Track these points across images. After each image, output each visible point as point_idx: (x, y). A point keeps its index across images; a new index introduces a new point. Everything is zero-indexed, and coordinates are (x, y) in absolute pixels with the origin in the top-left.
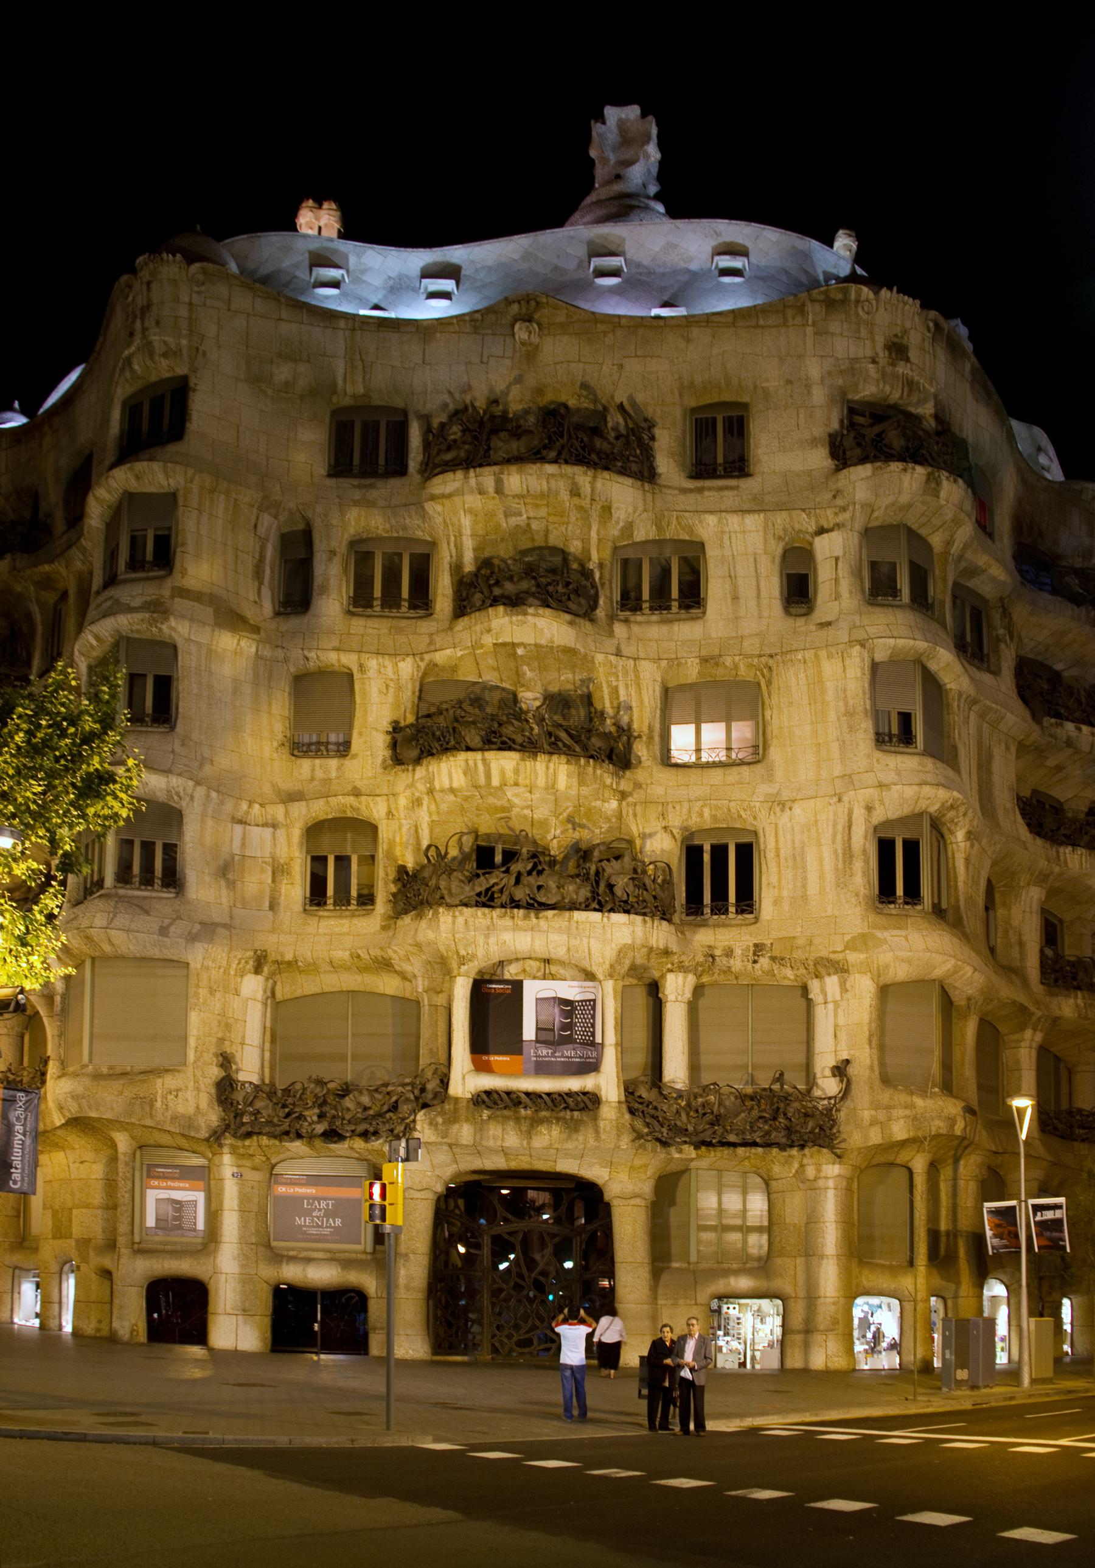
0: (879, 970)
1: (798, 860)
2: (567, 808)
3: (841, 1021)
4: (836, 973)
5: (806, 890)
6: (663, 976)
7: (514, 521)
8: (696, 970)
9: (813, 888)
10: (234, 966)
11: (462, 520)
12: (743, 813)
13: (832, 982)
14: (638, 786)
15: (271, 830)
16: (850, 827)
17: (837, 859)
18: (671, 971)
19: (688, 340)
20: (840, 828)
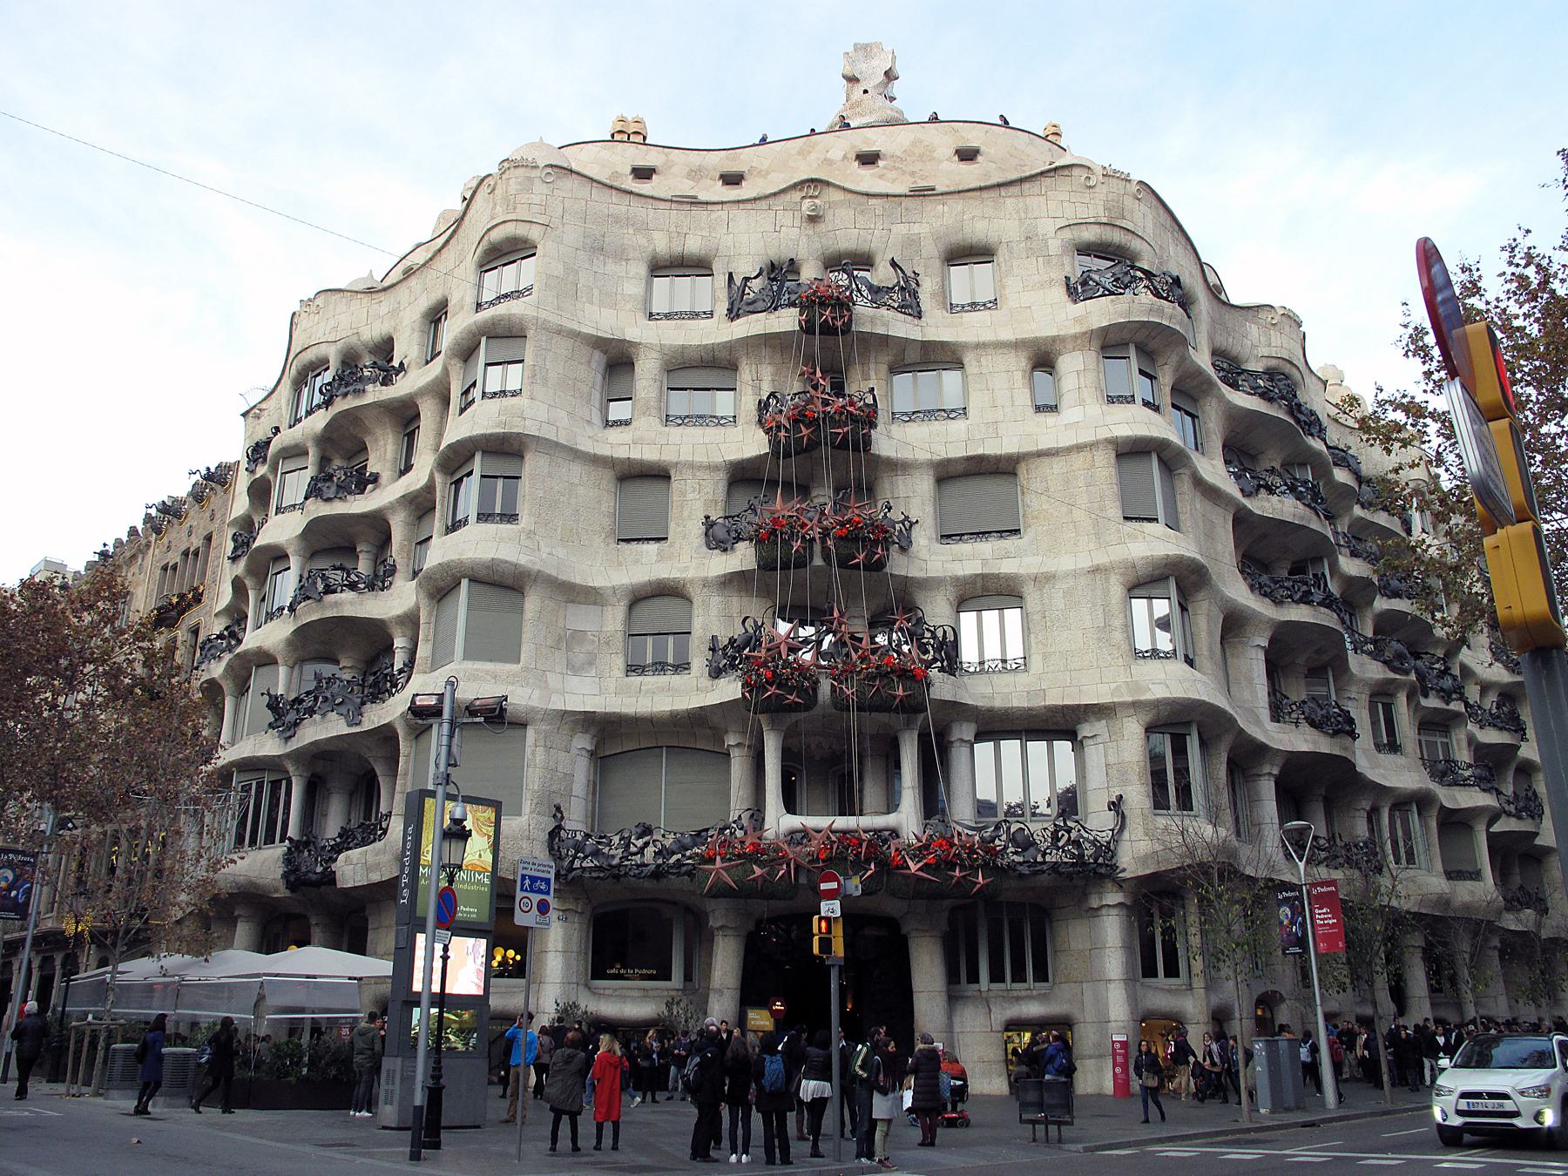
3: (1112, 760)
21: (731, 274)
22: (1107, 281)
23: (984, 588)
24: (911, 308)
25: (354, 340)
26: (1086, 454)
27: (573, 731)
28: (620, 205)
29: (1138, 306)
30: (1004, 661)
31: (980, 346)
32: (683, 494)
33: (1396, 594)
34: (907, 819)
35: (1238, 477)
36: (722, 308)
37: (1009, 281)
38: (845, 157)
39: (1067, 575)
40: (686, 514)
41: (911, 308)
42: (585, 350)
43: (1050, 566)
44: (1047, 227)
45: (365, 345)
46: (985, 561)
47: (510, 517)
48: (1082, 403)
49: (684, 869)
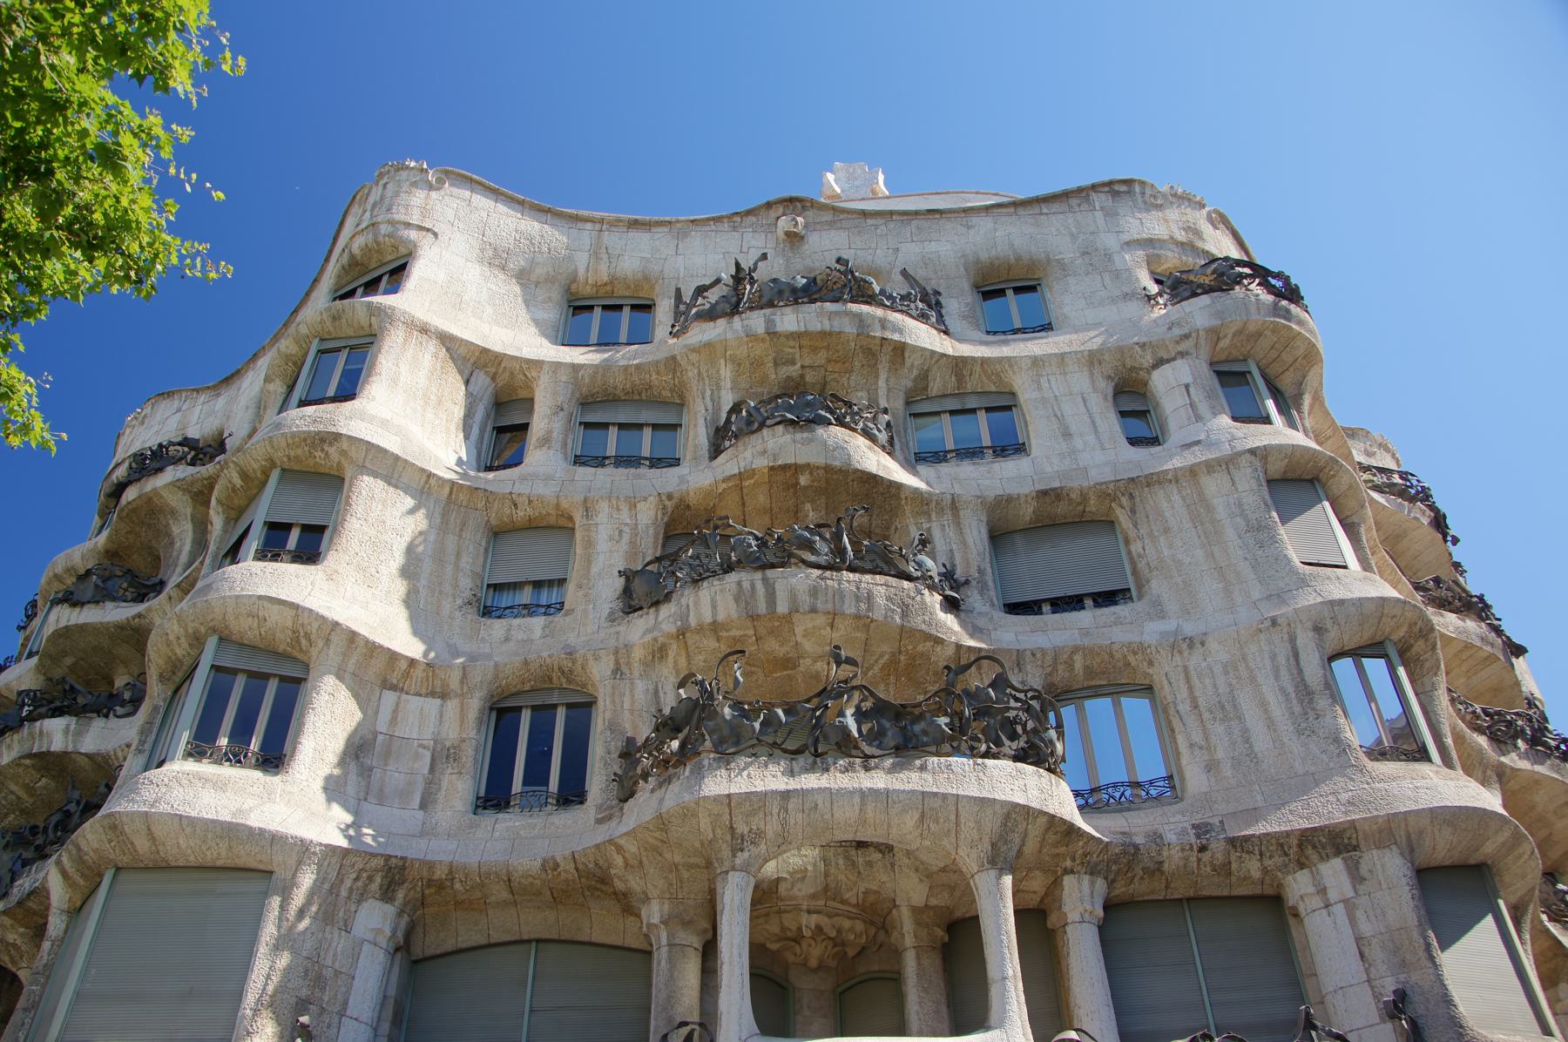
0: (1409, 837)
1: (1227, 710)
2: (881, 656)
3: (1366, 929)
4: (1338, 853)
5: (1251, 746)
6: (1057, 883)
8: (1109, 870)
9: (1262, 742)
10: (348, 883)
11: (722, 372)
12: (1131, 658)
13: (1333, 871)
15: (438, 701)
16: (1296, 656)
17: (1288, 700)
18: (1067, 871)
20: (1282, 660)
21: (678, 291)
23: (1089, 671)
27: (362, 897)
28: (532, 226)
30: (1136, 785)
31: (1036, 362)
32: (589, 544)
40: (594, 570)
44: (1110, 241)
46: (1085, 633)
48: (1198, 418)
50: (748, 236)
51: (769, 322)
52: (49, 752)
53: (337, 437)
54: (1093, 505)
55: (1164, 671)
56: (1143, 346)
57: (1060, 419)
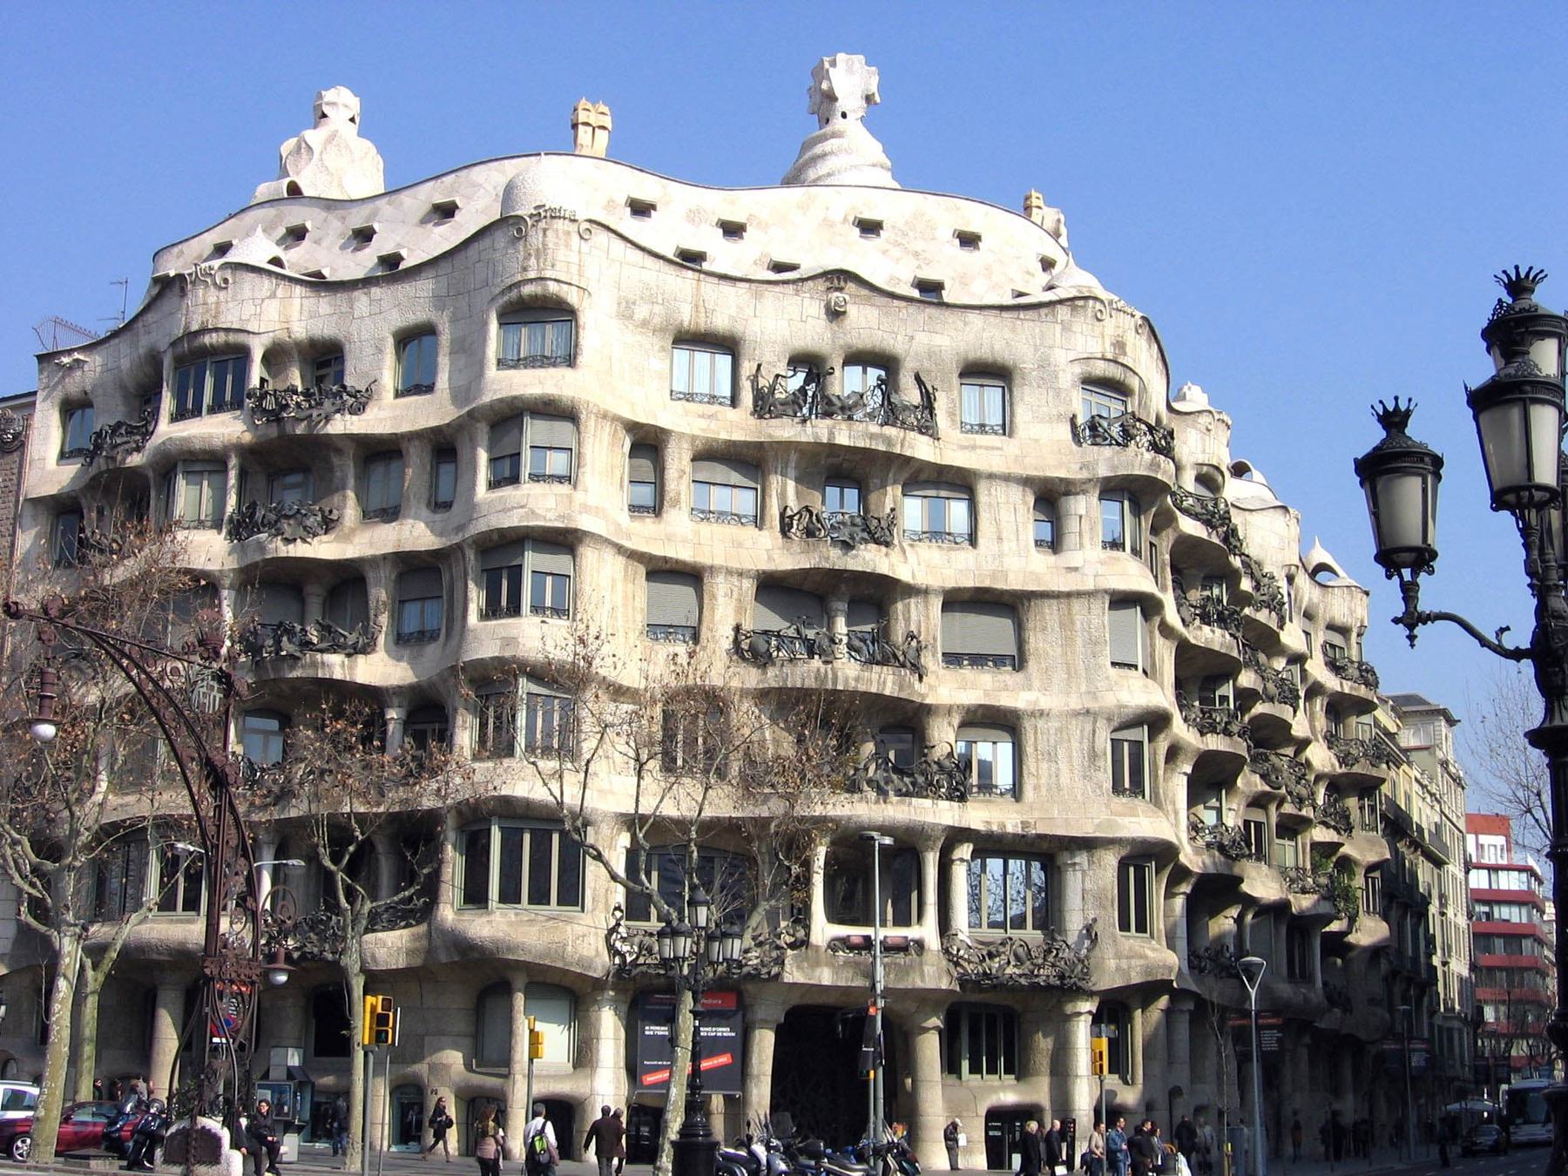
1: (1052, 757)
3: (1088, 886)
7: (831, 460)
9: (1065, 779)
13: (1082, 858)
14: (931, 687)
19: (966, 324)
22: (1115, 430)
23: (984, 716)
24: (927, 428)
25: (283, 336)
26: (1084, 601)
29: (1138, 460)
31: (991, 476)
32: (714, 597)
33: (1271, 700)
34: (926, 930)
35: (1179, 606)
36: (747, 397)
37: (1020, 410)
38: (845, 219)
39: (1061, 715)
40: (717, 617)
41: (927, 428)
42: (622, 433)
43: (1045, 703)
44: (1060, 357)
45: (298, 344)
47: (559, 612)
49: (745, 970)
50: (807, 302)
51: (831, 433)
52: (331, 680)
53: (576, 530)
54: (1005, 599)
55: (1027, 725)
56: (1061, 480)
57: (997, 522)
